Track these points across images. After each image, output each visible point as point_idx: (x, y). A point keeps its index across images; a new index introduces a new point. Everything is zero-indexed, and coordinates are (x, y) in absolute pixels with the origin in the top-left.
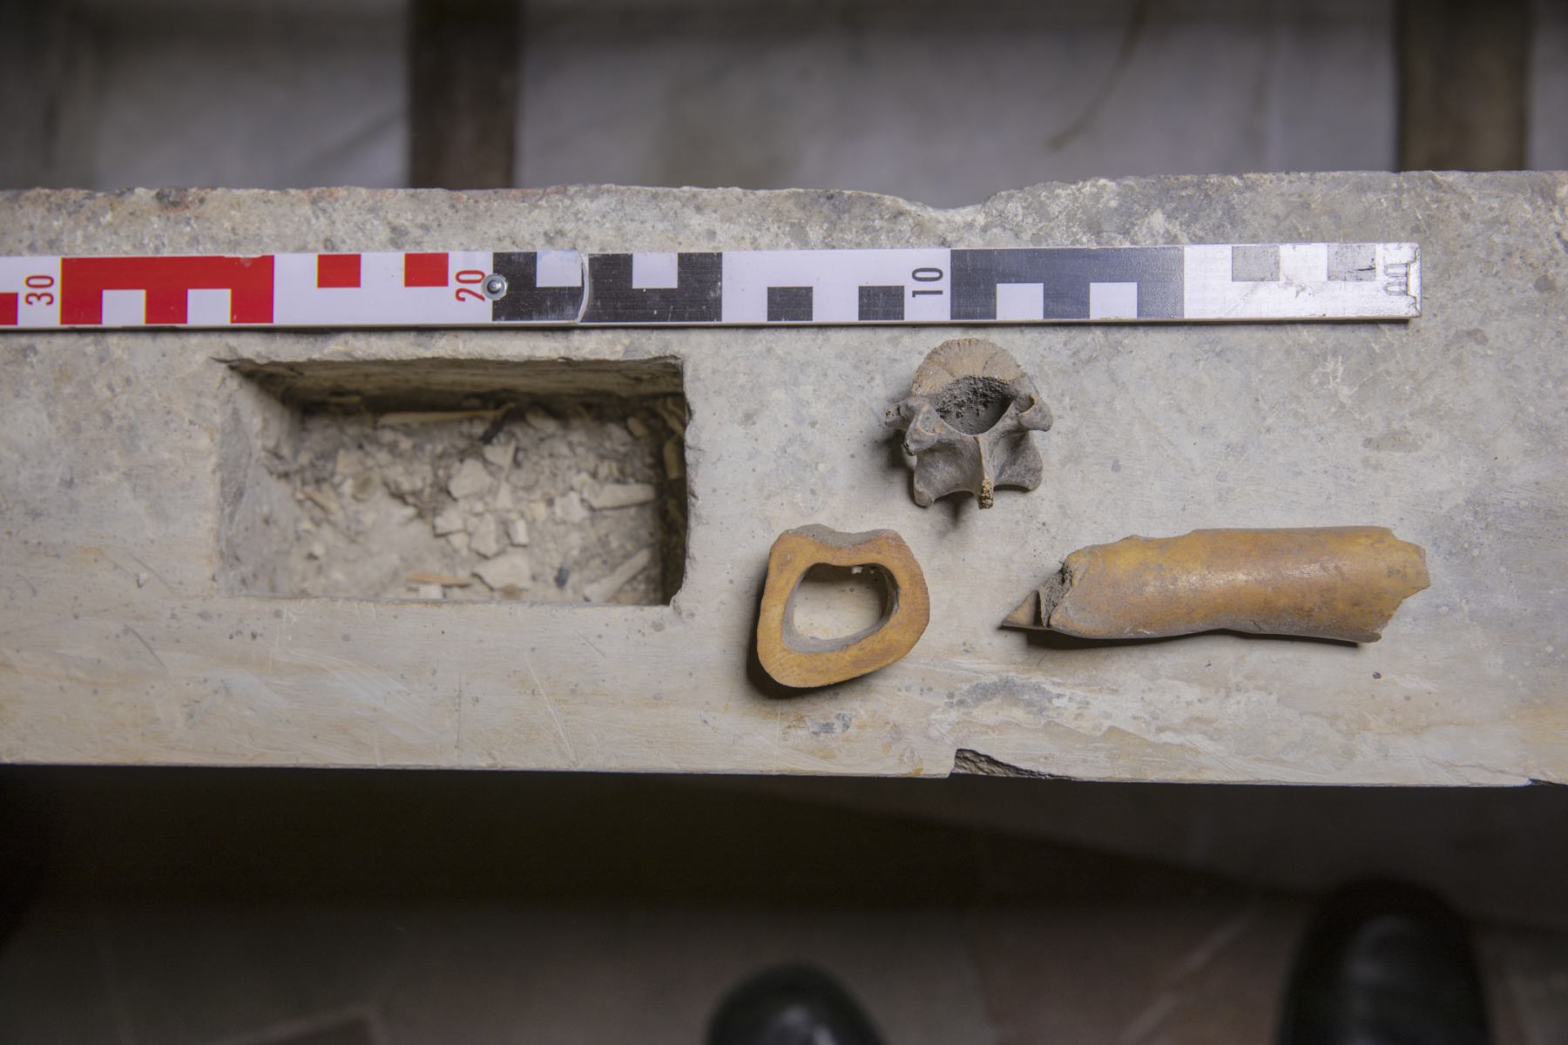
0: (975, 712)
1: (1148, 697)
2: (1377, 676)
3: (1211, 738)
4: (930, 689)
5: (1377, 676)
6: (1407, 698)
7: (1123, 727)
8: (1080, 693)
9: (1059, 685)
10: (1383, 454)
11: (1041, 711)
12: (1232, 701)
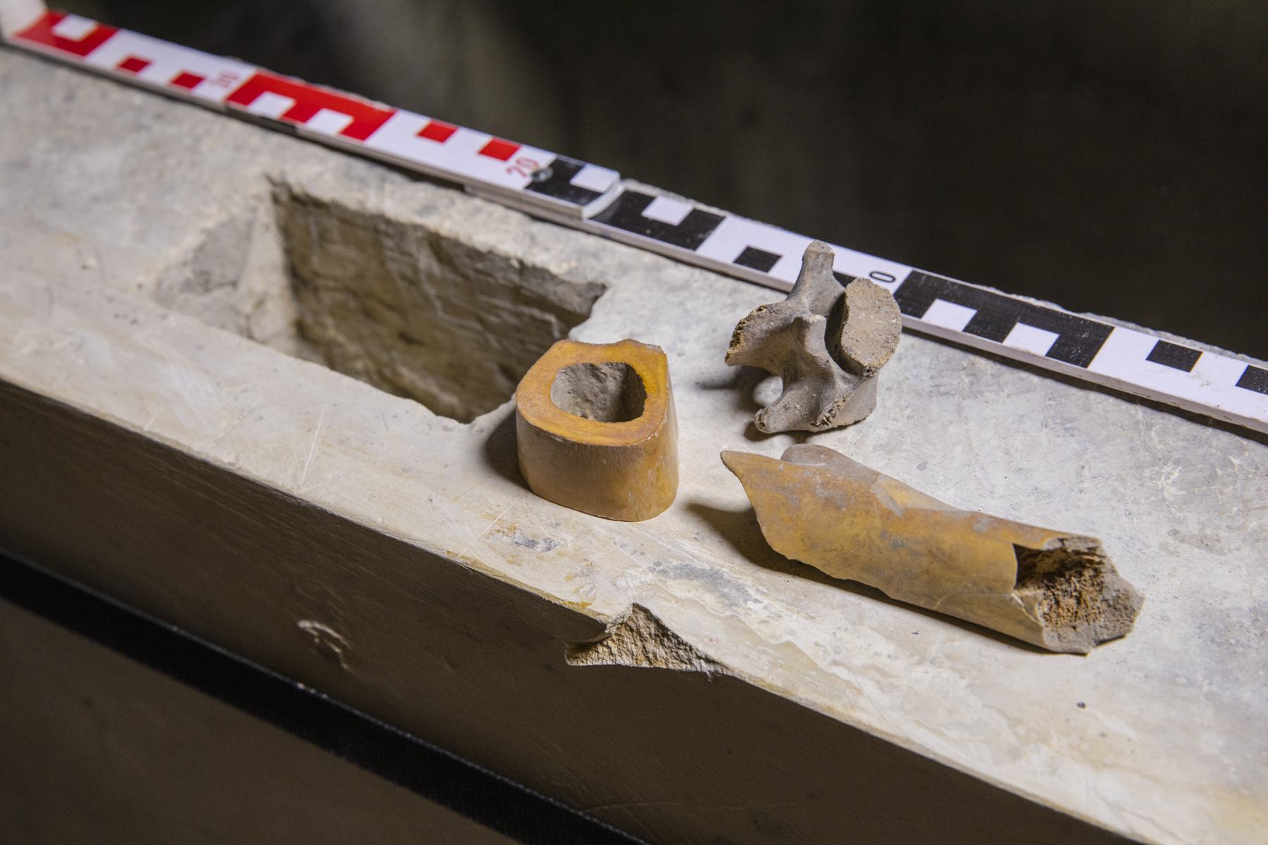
0: (670, 582)
1: (839, 634)
2: (1082, 705)
3: (882, 689)
4: (642, 554)
5: (1082, 705)
6: (1103, 735)
7: (800, 646)
8: (777, 607)
9: (763, 593)
10: (1184, 547)
11: (731, 605)
12: (921, 668)
